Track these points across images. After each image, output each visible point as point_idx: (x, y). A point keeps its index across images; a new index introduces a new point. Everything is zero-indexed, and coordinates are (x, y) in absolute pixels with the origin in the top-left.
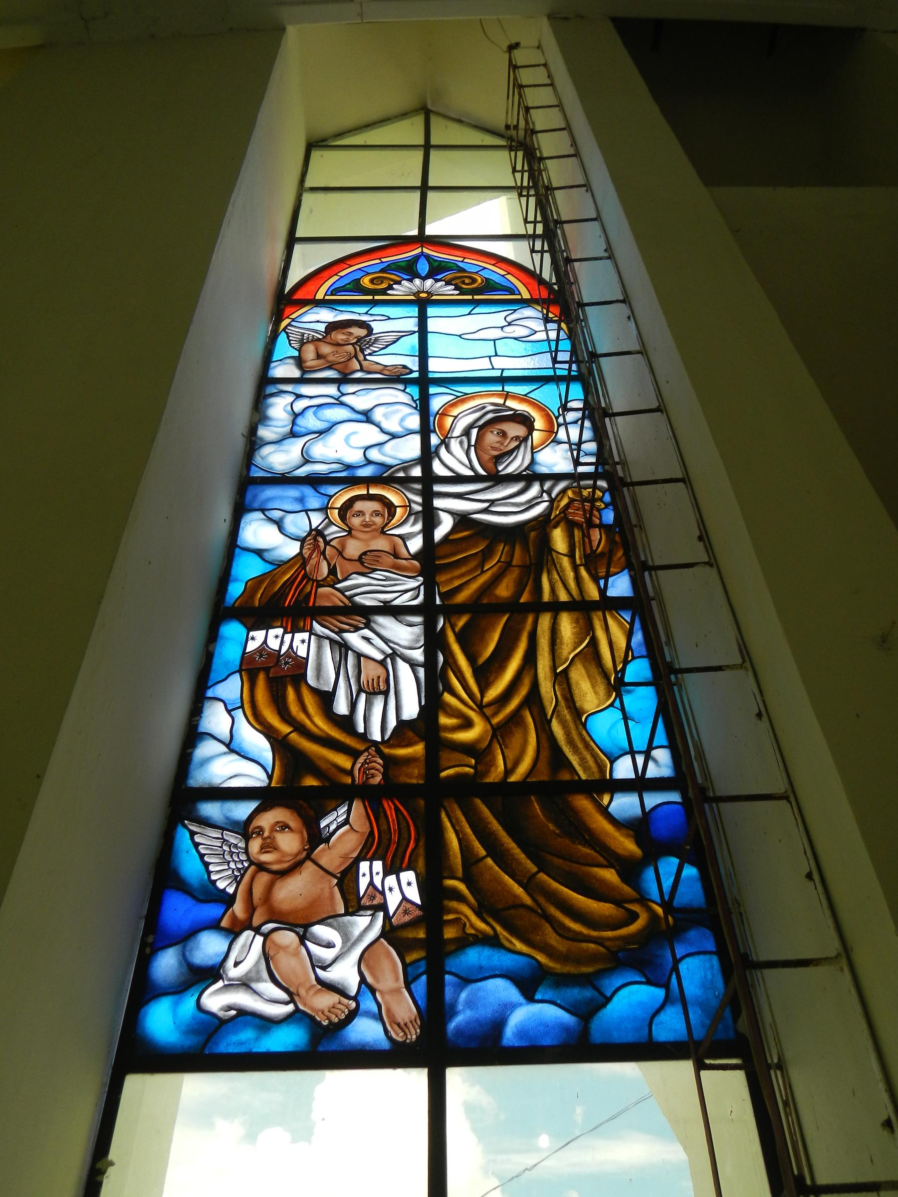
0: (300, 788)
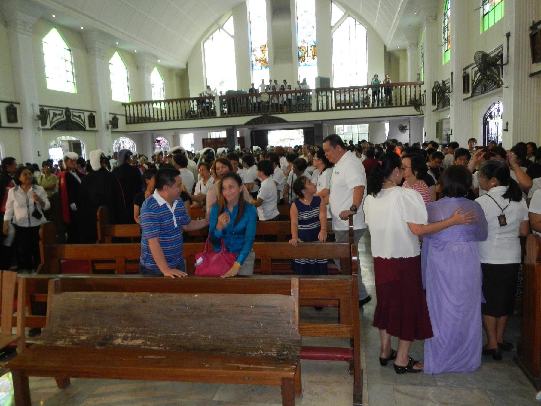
0: (257, 61)
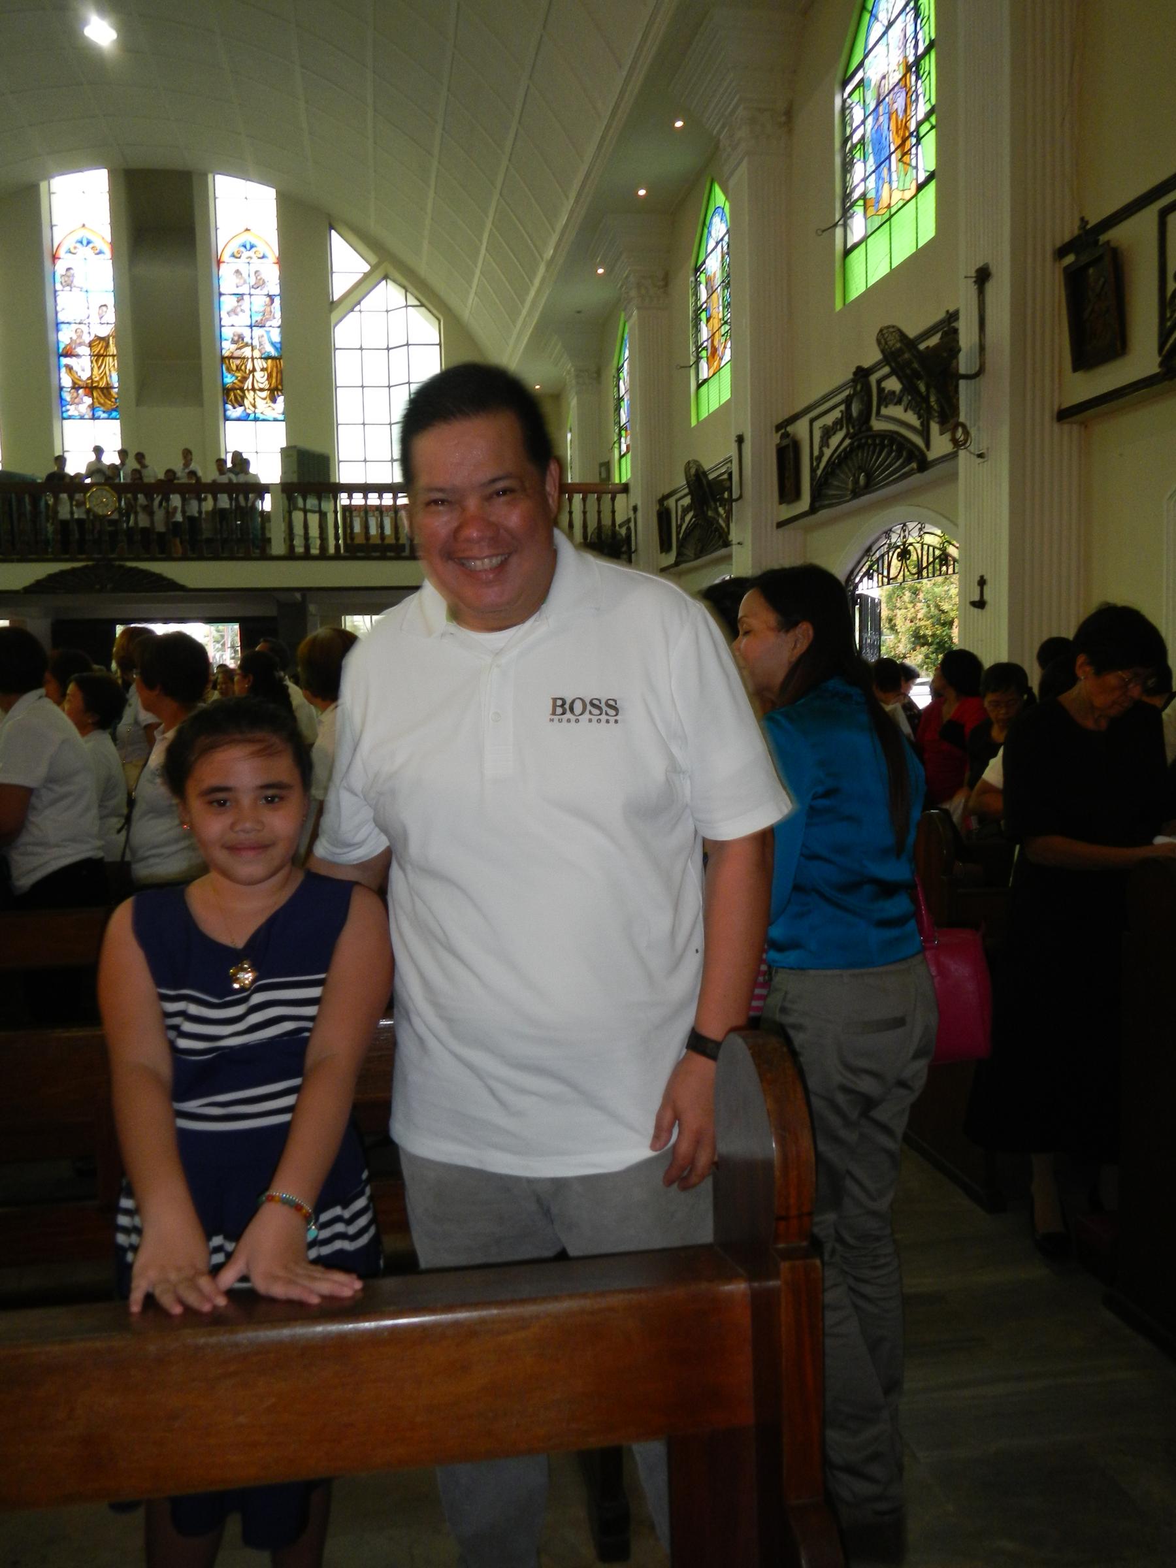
0: (76, 387)
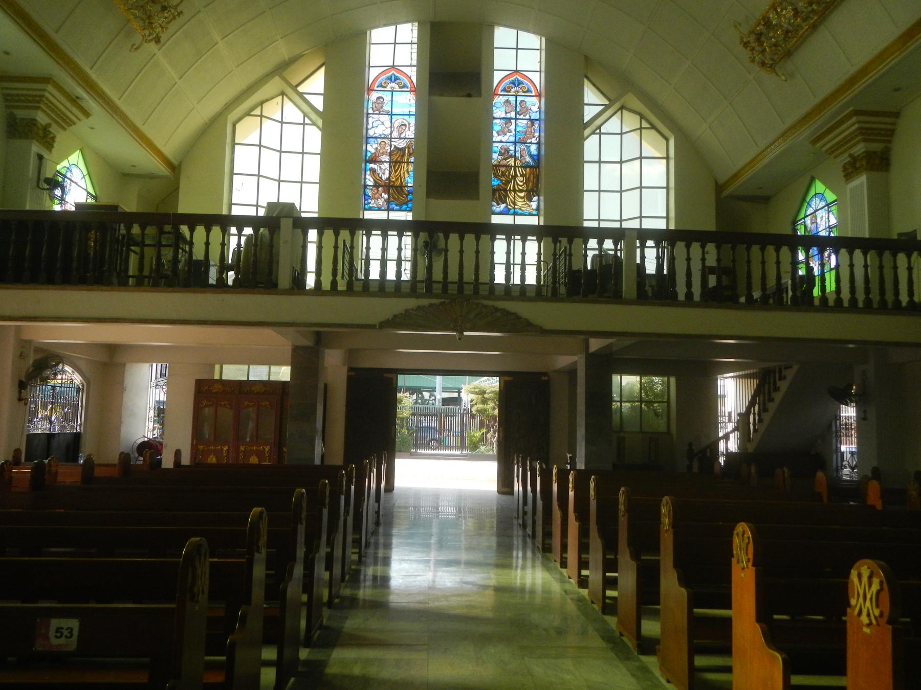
0: (376, 185)
